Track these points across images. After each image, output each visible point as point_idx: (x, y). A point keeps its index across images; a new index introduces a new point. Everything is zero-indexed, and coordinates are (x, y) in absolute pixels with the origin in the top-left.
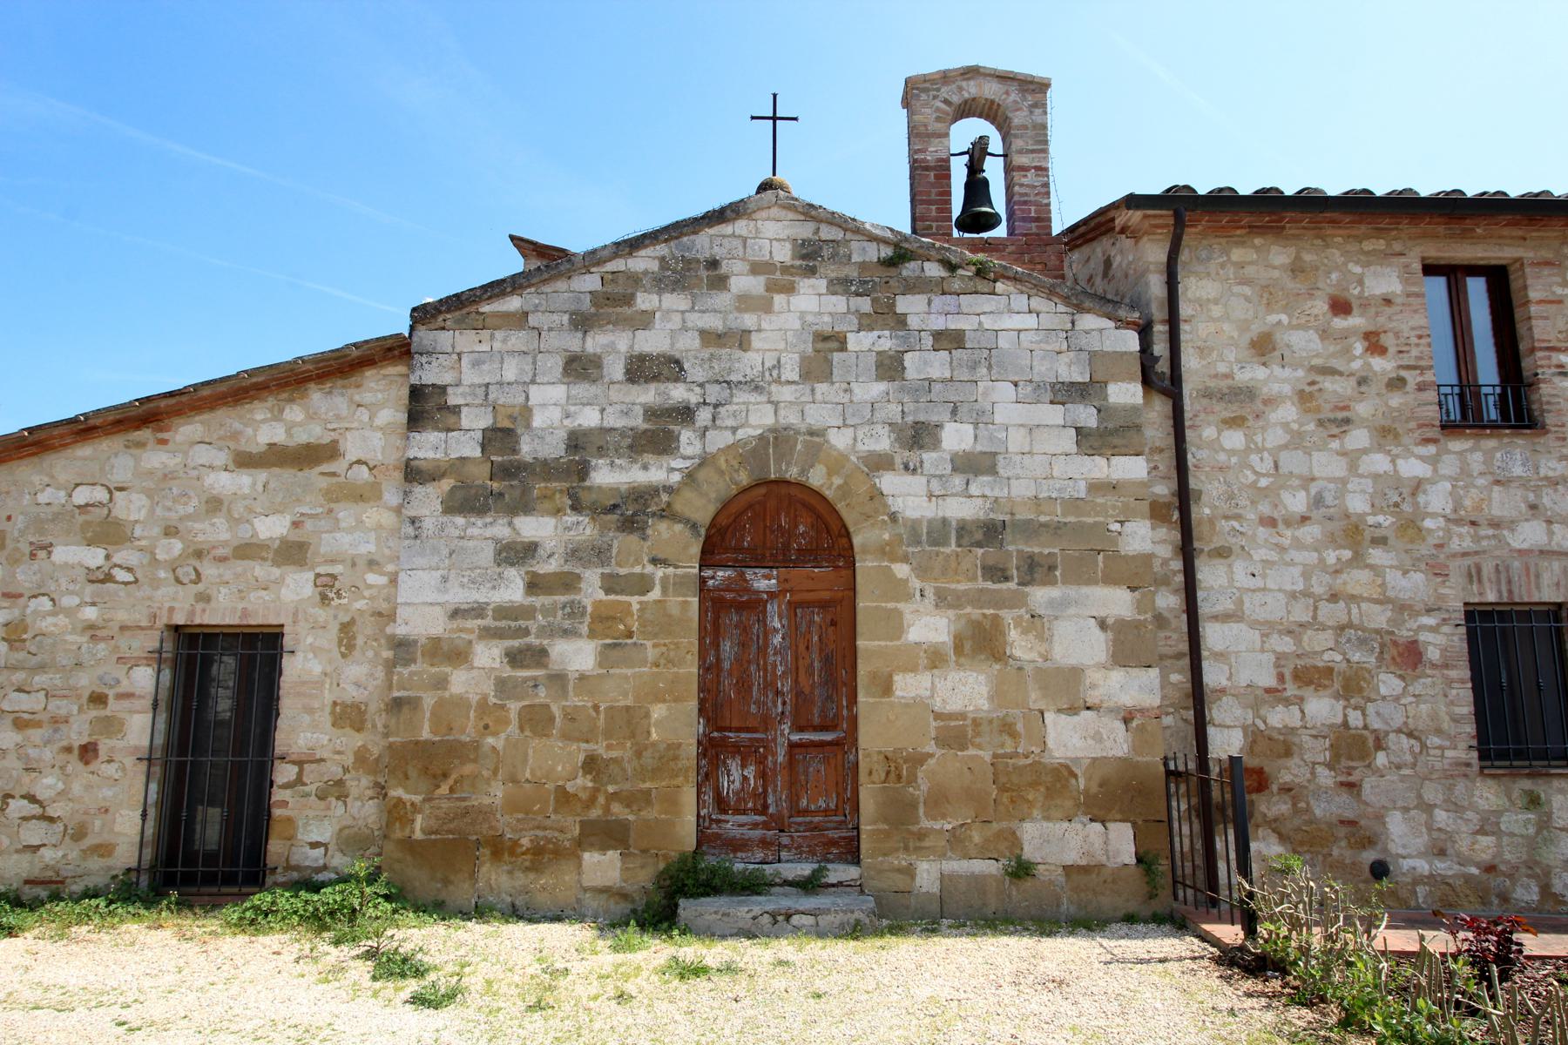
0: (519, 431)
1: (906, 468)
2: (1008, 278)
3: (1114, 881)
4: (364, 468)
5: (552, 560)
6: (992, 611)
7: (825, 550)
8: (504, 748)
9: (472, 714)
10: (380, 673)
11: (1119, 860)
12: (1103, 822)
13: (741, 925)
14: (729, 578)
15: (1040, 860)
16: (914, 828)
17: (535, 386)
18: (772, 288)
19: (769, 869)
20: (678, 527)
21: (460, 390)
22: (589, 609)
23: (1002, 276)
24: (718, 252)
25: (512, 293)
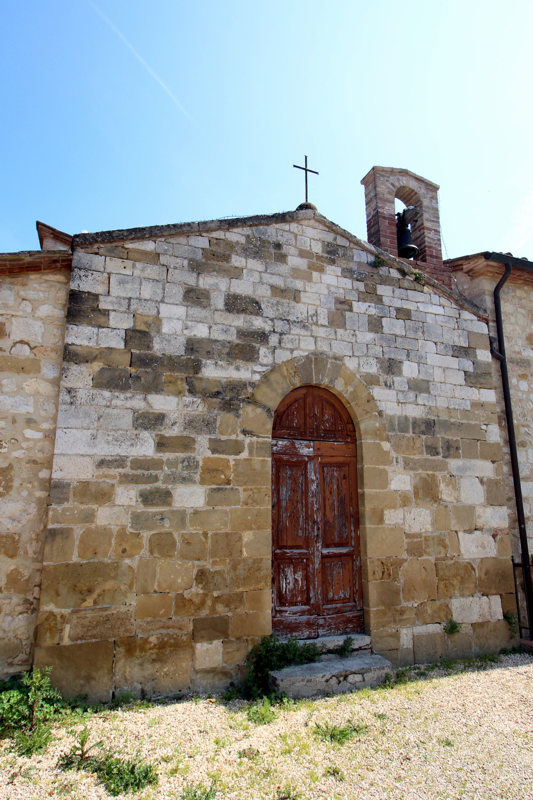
0: (152, 334)
1: (386, 385)
2: (430, 285)
3: (494, 631)
4: (26, 347)
5: (175, 427)
6: (431, 472)
7: (339, 431)
8: (138, 566)
9: (113, 541)
10: (33, 509)
11: (496, 617)
12: (487, 596)
13: (319, 687)
14: (286, 446)
15: (461, 622)
16: (398, 608)
17: (164, 304)
18: (312, 267)
19: (318, 642)
20: (259, 410)
21: (109, 299)
22: (201, 464)
23: (427, 284)
24: (281, 240)
25: (149, 239)
